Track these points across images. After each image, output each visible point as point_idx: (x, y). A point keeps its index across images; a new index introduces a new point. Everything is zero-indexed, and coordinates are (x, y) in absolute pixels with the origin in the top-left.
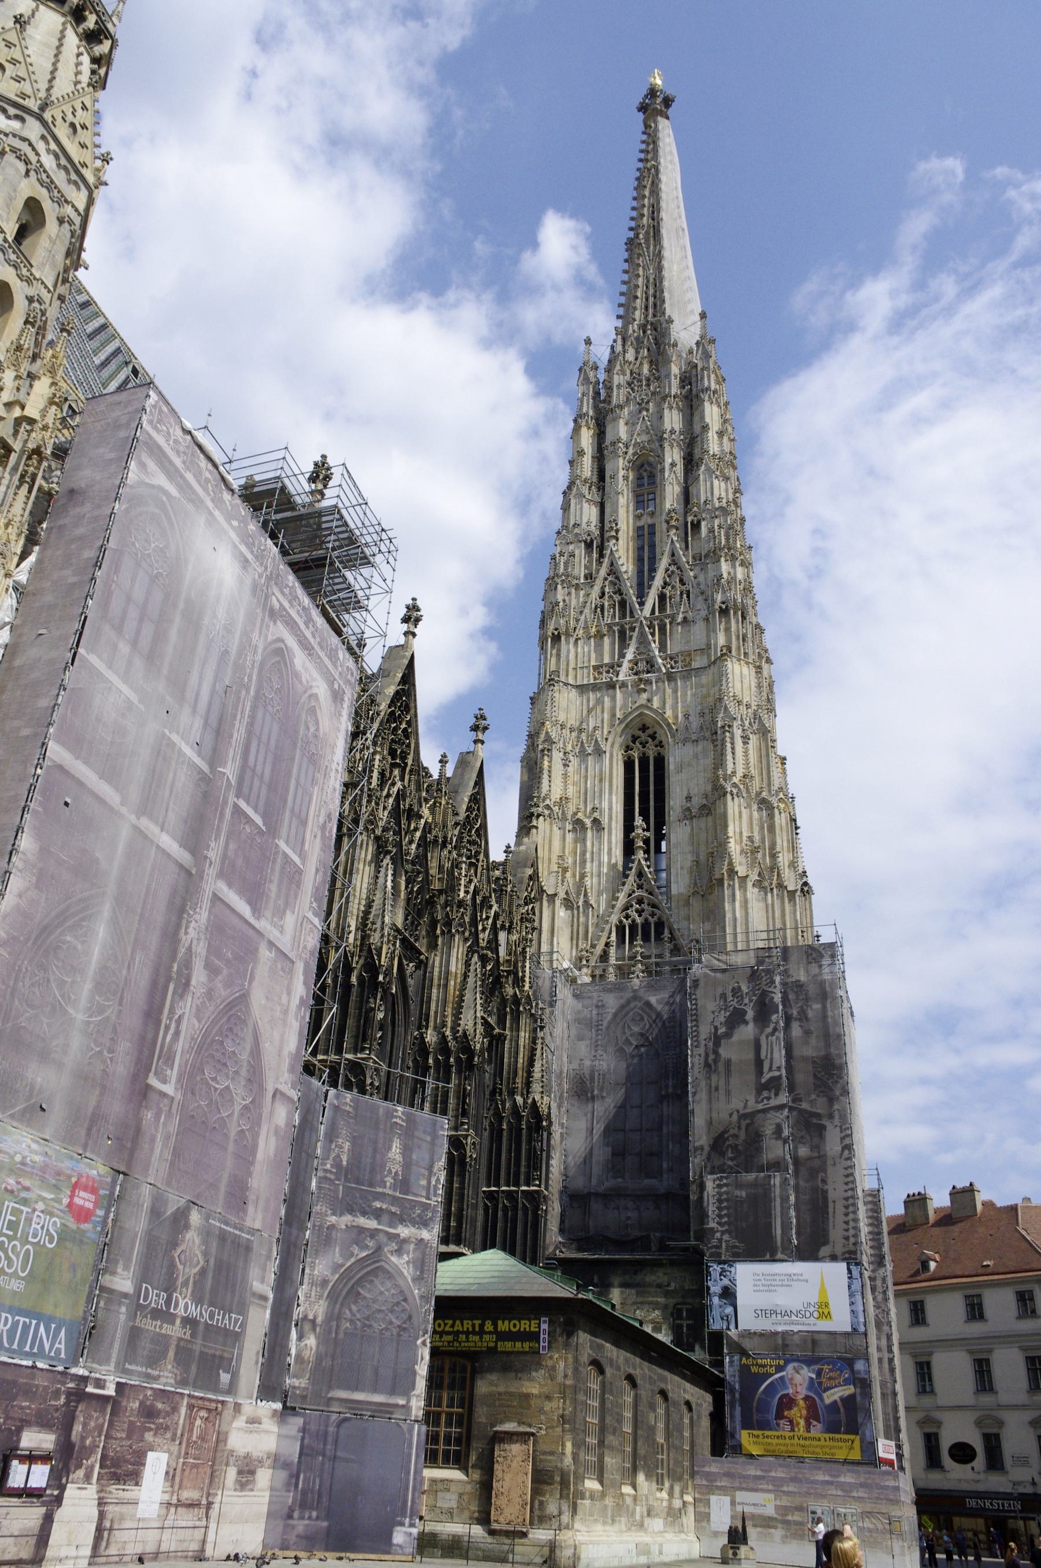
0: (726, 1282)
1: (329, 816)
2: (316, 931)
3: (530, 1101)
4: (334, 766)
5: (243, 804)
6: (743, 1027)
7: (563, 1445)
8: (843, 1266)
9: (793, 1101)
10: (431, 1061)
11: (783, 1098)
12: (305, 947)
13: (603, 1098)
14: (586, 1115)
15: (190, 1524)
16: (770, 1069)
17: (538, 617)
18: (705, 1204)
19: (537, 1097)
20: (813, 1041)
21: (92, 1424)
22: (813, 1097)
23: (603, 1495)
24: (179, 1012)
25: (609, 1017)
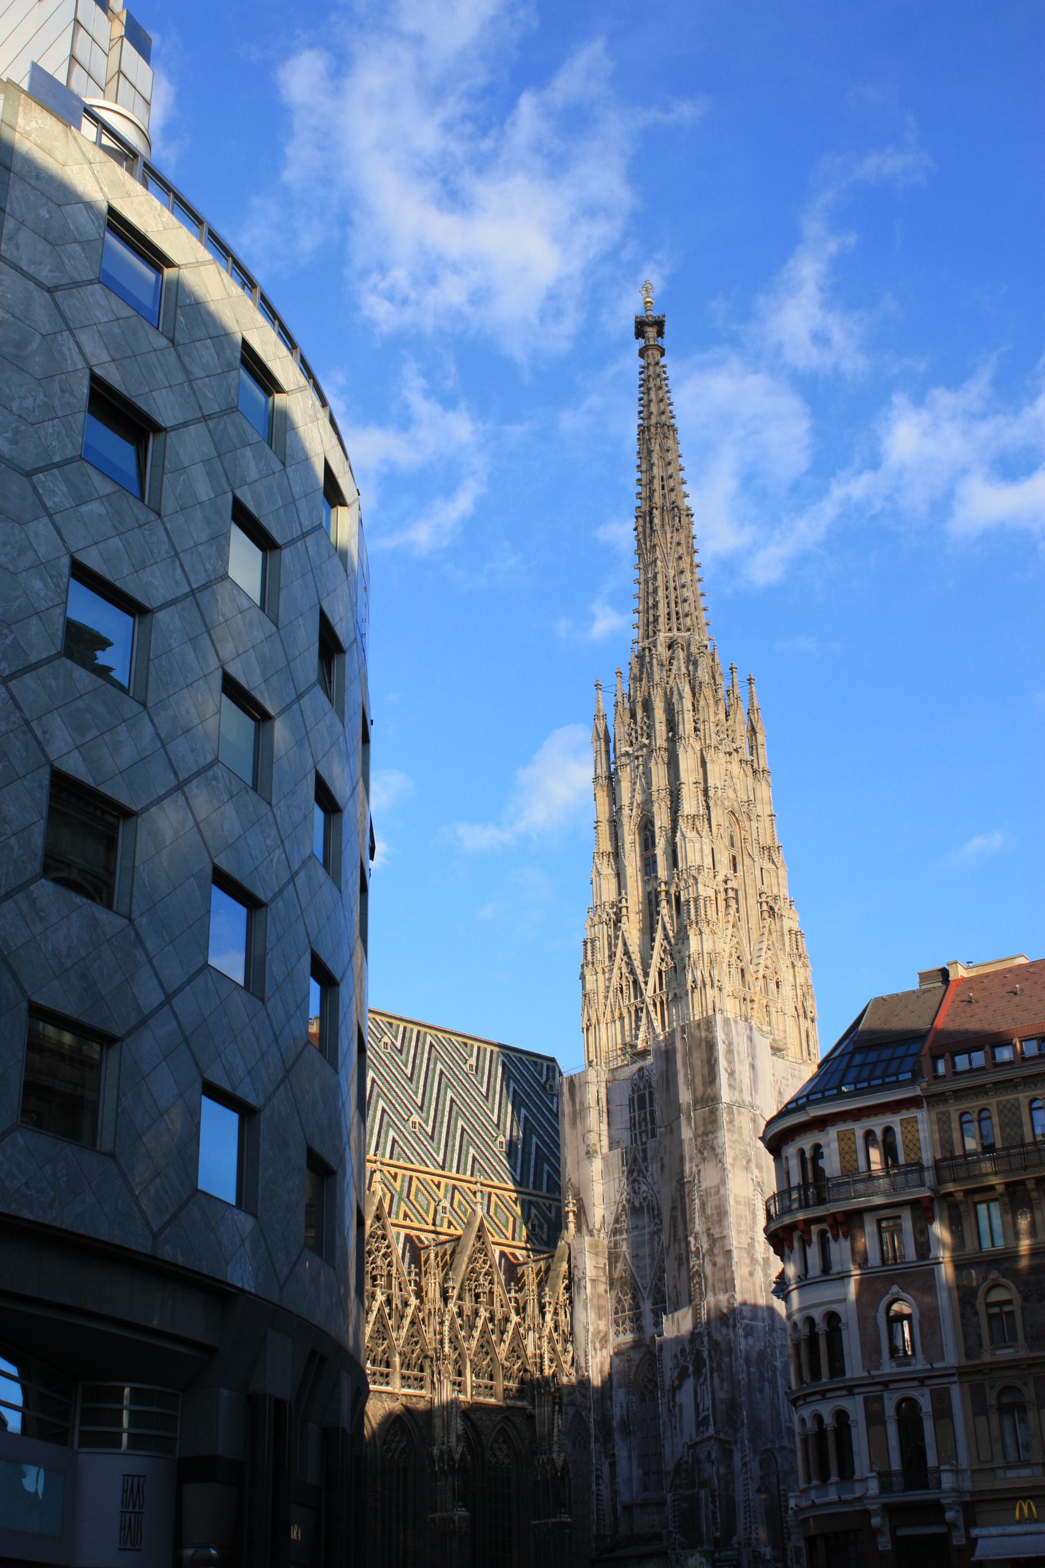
9: (717, 1432)
10: (437, 1468)
11: (711, 1431)
16: (703, 1411)
19: (555, 1455)
20: (725, 1385)
22: (726, 1429)
25: (634, 1369)
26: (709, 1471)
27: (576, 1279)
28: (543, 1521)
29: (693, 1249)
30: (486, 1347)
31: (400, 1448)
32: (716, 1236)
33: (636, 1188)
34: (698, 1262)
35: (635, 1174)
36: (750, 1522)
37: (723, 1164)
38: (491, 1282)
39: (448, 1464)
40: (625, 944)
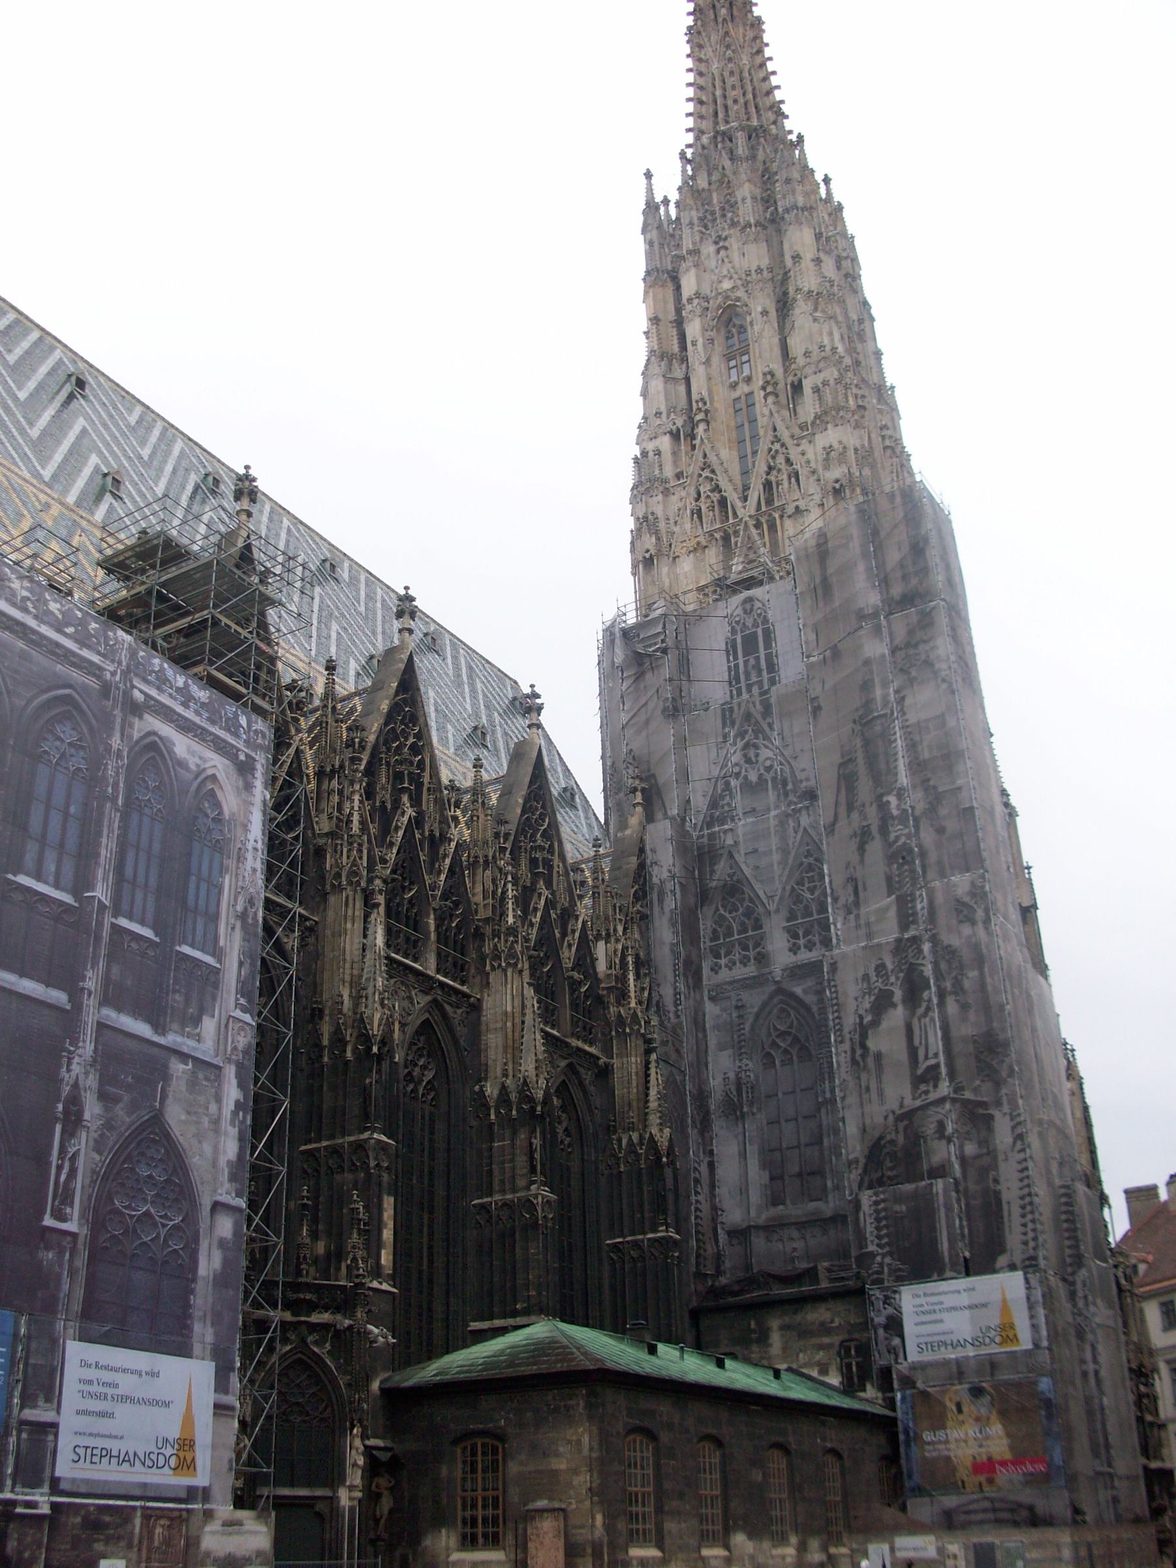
0: (890, 1310)
1: (251, 902)
3: (647, 1136)
4: (250, 846)
5: (124, 922)
6: (891, 1011)
7: (593, 1518)
8: (1019, 1274)
9: (955, 1091)
10: (493, 1117)
11: (945, 1088)
12: (235, 1048)
13: (753, 1114)
14: (736, 1136)
16: (926, 1058)
17: (629, 538)
18: (862, 1225)
19: (654, 1131)
20: (972, 1016)
21: (29, 1539)
22: (978, 1082)
23: (665, 1561)
24: (72, 1150)
25: (751, 1019)
26: (941, 1152)
27: (655, 880)
29: (895, 812)
30: (547, 944)
31: (426, 1080)
32: (940, 789)
33: (752, 754)
34: (906, 831)
36: (1034, 1230)
37: (951, 684)
38: (551, 850)
39: (519, 1109)
40: (705, 456)
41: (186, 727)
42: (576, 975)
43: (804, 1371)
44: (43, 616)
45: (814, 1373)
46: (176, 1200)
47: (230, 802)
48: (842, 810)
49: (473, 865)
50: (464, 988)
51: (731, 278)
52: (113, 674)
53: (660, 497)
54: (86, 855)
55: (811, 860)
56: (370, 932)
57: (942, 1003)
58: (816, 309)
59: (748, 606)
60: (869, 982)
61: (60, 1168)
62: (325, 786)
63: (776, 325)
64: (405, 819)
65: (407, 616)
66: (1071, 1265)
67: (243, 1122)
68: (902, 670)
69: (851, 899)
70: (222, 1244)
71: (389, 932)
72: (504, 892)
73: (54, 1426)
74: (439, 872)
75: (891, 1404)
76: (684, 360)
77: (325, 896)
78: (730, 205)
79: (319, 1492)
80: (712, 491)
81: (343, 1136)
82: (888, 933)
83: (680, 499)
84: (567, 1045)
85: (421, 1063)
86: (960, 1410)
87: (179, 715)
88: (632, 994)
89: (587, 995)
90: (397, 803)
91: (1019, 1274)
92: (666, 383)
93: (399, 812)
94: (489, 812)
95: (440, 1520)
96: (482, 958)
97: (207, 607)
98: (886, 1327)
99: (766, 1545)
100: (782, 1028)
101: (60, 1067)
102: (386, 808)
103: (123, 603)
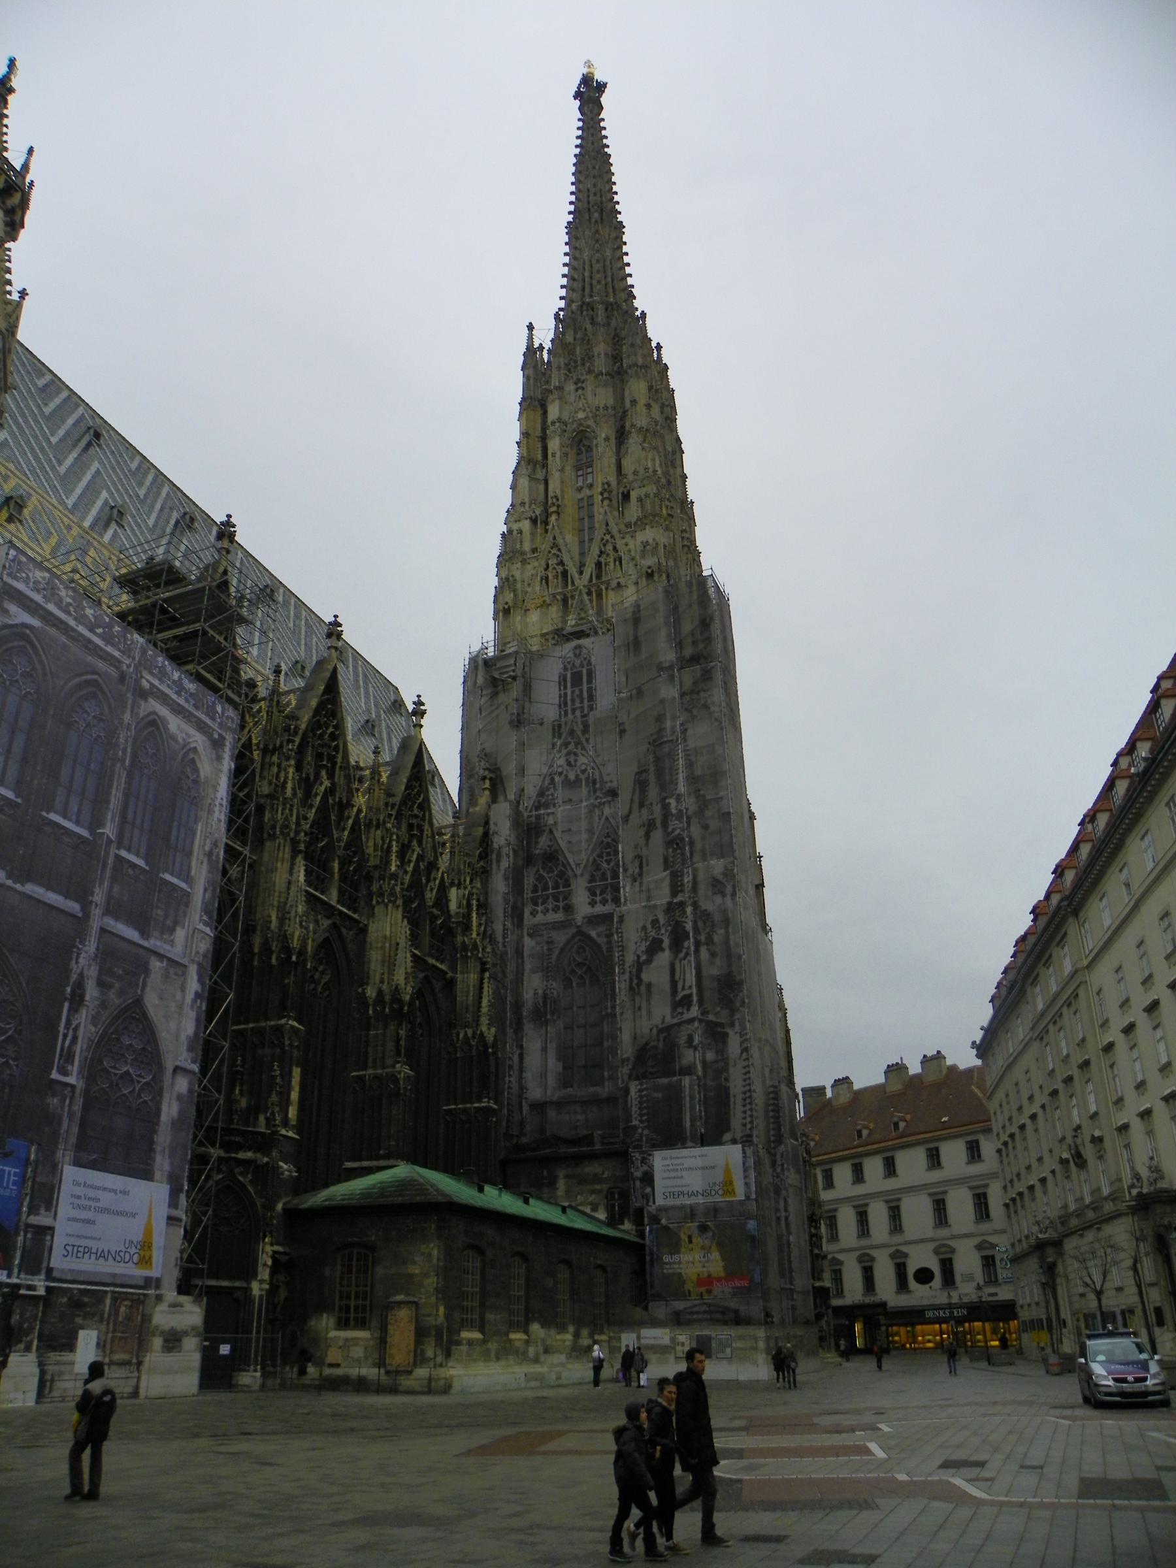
0: (645, 1168)
1: (215, 844)
2: (207, 938)
5: (124, 853)
6: (660, 954)
7: (438, 1310)
8: (739, 1146)
9: (702, 1014)
10: (371, 1012)
11: (695, 1011)
12: (197, 952)
15: (124, 1376)
16: (683, 989)
17: (493, 592)
19: (484, 1028)
20: (718, 961)
21: (28, 1314)
22: (719, 1009)
23: (484, 1341)
24: (75, 1023)
25: (556, 953)
26: (689, 1057)
27: (495, 846)
28: (460, 1106)
29: (674, 811)
30: (416, 887)
31: (323, 982)
32: (708, 798)
33: (572, 759)
34: (681, 825)
35: (571, 747)
36: (751, 1116)
37: (721, 723)
38: (423, 819)
39: (391, 1009)
40: (554, 538)
41: (178, 710)
42: (435, 911)
43: (581, 1208)
44: (81, 619)
45: (588, 1210)
46: (148, 1064)
47: (205, 768)
48: (636, 805)
49: (369, 825)
50: (356, 916)
51: (584, 410)
52: (128, 666)
53: (519, 565)
54: (100, 801)
55: (609, 840)
56: (295, 870)
57: (697, 951)
58: (644, 441)
59: (577, 652)
60: (646, 933)
61: (65, 1036)
62: (267, 760)
63: (614, 449)
64: (322, 788)
65: (334, 637)
66: (774, 1142)
67: (200, 1008)
68: (686, 710)
69: (637, 870)
70: (179, 1097)
71: (308, 872)
72: (390, 846)
73: (52, 1229)
74: (344, 829)
75: (641, 1234)
76: (545, 466)
77: (261, 842)
78: (589, 357)
79: (237, 1284)
80: (558, 564)
81: (266, 1021)
82: (663, 897)
83: (534, 568)
84: (425, 962)
85: (321, 968)
86: (690, 1241)
87: (172, 700)
88: (474, 928)
89: (442, 926)
90: (317, 776)
91: (739, 1146)
92: (530, 481)
93: (318, 783)
94: (383, 787)
95: (322, 1307)
96: (370, 895)
97: (199, 621)
98: (642, 1180)
99: (553, 1332)
100: (580, 960)
101: (71, 960)
102: (309, 779)
103: (131, 611)
